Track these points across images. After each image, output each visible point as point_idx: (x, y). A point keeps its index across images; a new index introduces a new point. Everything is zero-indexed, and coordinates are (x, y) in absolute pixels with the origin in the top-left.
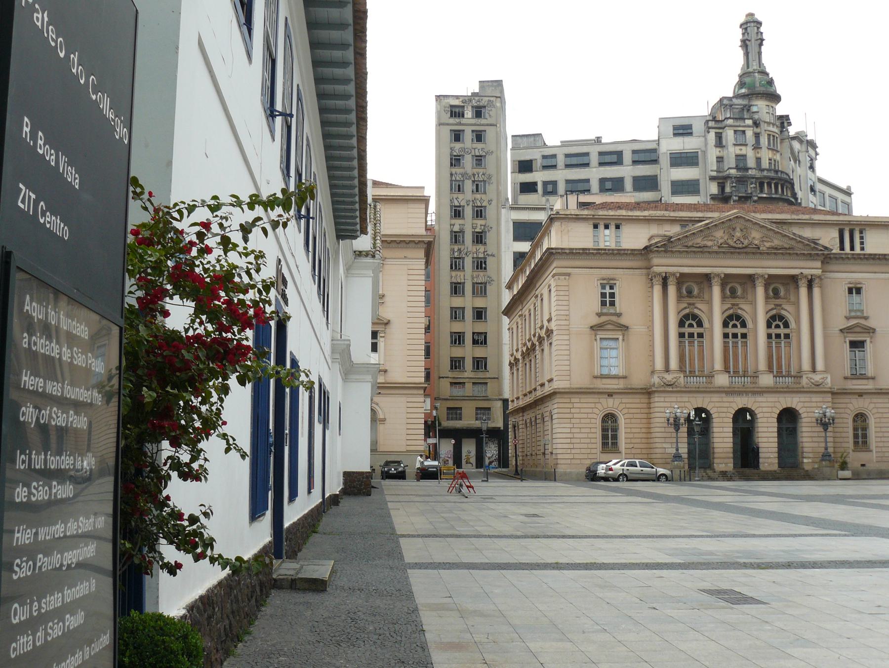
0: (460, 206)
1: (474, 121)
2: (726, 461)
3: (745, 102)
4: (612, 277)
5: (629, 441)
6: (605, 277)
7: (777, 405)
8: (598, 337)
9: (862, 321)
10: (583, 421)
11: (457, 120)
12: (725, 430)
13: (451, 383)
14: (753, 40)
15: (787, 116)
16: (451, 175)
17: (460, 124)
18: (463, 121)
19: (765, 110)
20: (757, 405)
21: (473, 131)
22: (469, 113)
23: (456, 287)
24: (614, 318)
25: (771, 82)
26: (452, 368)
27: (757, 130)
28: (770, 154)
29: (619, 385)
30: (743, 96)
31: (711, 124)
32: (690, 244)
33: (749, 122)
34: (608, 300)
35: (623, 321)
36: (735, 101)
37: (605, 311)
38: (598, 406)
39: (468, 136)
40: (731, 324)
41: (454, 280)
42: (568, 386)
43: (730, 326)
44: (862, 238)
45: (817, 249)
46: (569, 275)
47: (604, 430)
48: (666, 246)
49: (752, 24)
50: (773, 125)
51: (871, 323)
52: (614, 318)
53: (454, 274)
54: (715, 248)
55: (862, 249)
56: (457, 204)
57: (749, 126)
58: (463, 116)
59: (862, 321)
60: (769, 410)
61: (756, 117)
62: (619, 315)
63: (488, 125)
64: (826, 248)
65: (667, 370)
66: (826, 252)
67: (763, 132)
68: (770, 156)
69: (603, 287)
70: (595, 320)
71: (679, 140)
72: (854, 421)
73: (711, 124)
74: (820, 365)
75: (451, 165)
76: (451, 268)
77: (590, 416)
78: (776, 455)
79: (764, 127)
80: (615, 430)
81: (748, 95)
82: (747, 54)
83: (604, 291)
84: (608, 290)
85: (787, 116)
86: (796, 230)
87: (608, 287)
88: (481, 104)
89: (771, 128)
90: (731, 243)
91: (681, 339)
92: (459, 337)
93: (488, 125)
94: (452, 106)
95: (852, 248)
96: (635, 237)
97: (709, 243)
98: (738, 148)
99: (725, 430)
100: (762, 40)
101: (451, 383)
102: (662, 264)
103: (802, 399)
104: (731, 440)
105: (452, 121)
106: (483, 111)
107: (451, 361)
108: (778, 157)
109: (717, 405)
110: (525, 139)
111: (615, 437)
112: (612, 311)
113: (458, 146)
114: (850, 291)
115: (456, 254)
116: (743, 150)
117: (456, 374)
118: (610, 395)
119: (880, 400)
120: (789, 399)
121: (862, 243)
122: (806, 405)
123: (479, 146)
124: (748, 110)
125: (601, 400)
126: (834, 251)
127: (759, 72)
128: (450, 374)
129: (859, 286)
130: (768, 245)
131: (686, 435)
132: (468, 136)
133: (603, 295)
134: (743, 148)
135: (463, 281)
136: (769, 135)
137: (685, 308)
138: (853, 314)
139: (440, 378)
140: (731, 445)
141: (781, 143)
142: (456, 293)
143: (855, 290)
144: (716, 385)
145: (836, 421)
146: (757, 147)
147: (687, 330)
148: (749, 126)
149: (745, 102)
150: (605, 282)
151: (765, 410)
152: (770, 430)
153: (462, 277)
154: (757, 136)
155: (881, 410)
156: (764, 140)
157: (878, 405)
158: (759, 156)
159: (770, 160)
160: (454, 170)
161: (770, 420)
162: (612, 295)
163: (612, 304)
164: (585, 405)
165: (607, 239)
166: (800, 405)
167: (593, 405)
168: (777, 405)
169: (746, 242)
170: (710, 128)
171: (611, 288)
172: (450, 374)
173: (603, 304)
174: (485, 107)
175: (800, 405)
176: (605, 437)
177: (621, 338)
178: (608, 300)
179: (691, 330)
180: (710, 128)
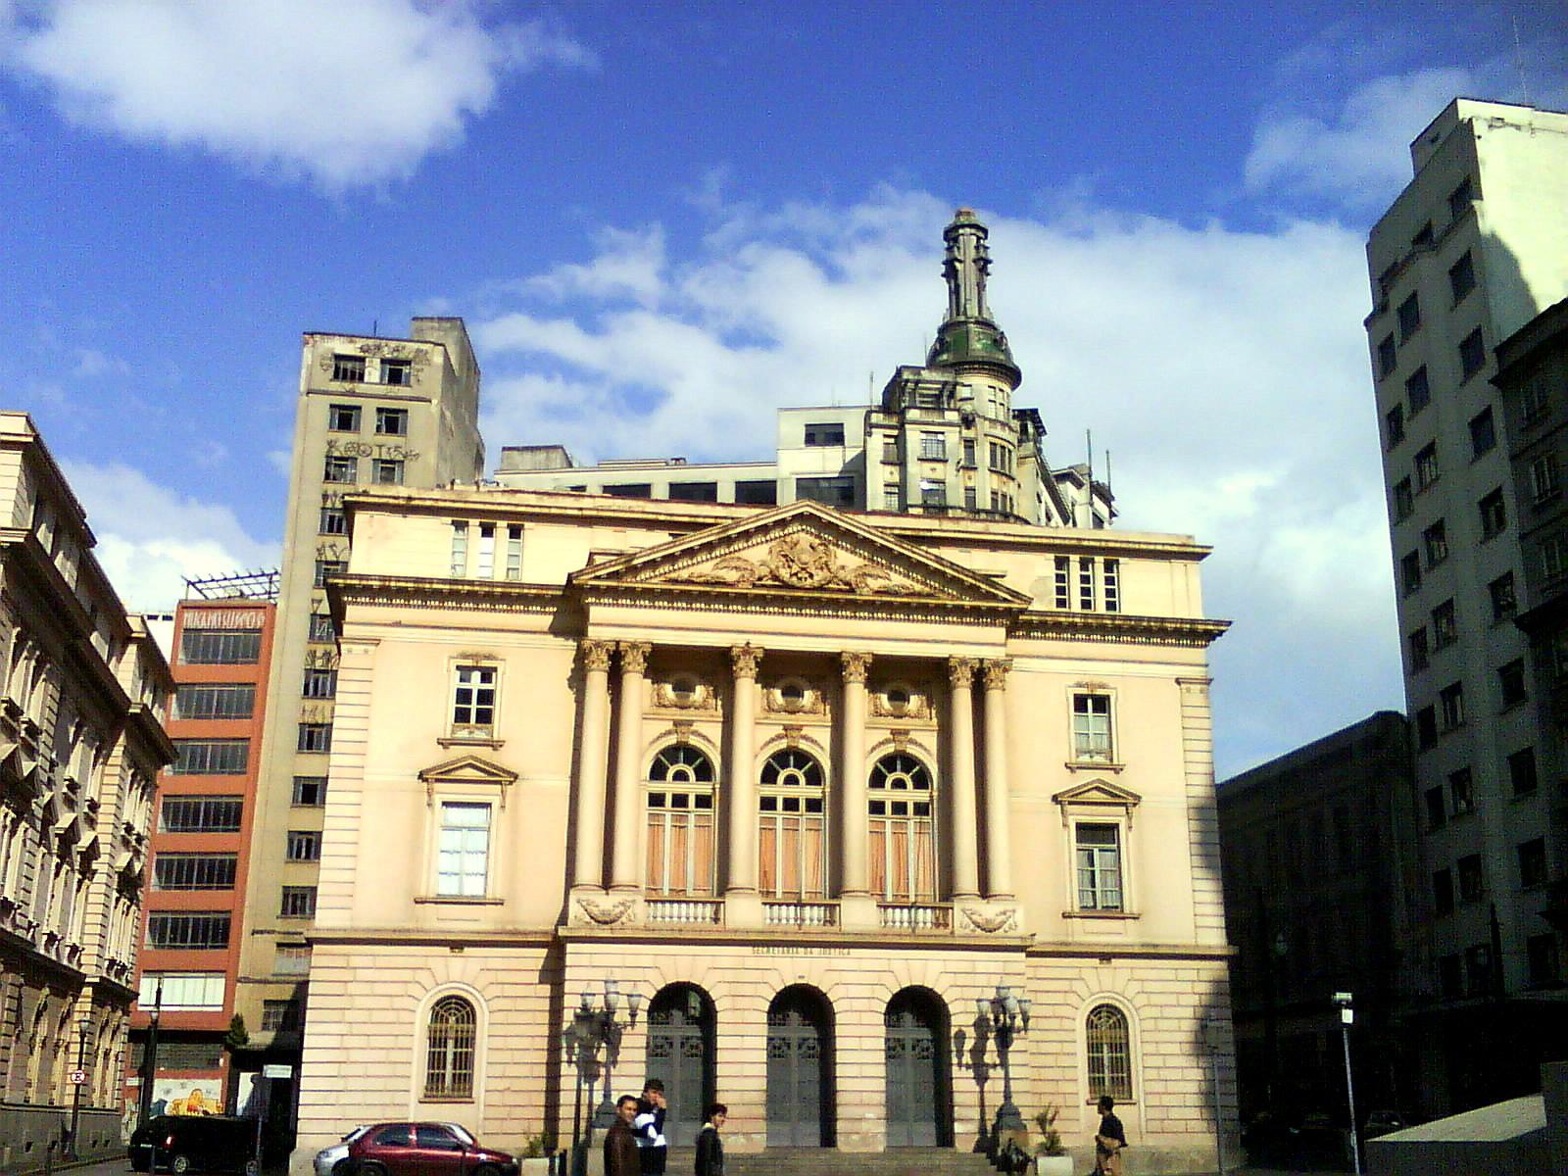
0: (337, 563)
1: (383, 389)
2: (748, 1127)
3: (948, 377)
4: (486, 651)
5: (498, 1070)
6: (470, 650)
7: (887, 979)
8: (438, 799)
9: (1108, 777)
10: (377, 1016)
11: (347, 386)
12: (749, 1042)
13: (279, 945)
14: (969, 261)
15: (1035, 411)
16: (325, 497)
17: (352, 394)
18: (360, 388)
19: (989, 394)
20: (835, 977)
21: (380, 410)
22: (373, 372)
23: (311, 734)
24: (485, 753)
25: (998, 341)
26: (284, 910)
27: (966, 433)
28: (994, 482)
29: (482, 921)
30: (944, 367)
31: (876, 418)
32: (684, 574)
33: (952, 416)
34: (475, 707)
35: (504, 759)
36: (926, 375)
37: (463, 734)
38: (423, 977)
39: (369, 419)
40: (783, 775)
41: (309, 720)
42: (347, 924)
43: (781, 778)
44: (1109, 581)
45: (995, 597)
46: (376, 642)
47: (437, 1041)
48: (622, 581)
49: (968, 230)
50: (1004, 424)
51: (1126, 782)
52: (485, 753)
53: (309, 704)
54: (744, 589)
55: (1111, 606)
56: (331, 557)
57: (951, 424)
58: (361, 378)
59: (1108, 777)
60: (866, 991)
61: (967, 407)
62: (496, 745)
63: (411, 399)
64: (1016, 594)
65: (607, 883)
66: (1016, 605)
67: (981, 438)
68: (995, 487)
69: (465, 672)
70: (436, 757)
71: (816, 452)
72: (1090, 1024)
73: (876, 418)
74: (1000, 882)
75: (327, 476)
76: (306, 692)
77: (398, 1003)
78: (882, 1112)
79: (983, 427)
80: (466, 1041)
81: (952, 365)
82: (955, 292)
83: (465, 686)
84: (475, 683)
85: (1035, 411)
86: (949, 554)
87: (476, 676)
88: (402, 356)
89: (998, 431)
90: (784, 574)
91: (656, 810)
92: (309, 842)
93: (411, 399)
94: (339, 357)
95: (1086, 604)
96: (552, 556)
97: (731, 576)
98: (928, 466)
99: (749, 1042)
100: (988, 262)
101: (279, 945)
102: (608, 621)
103: (952, 967)
104: (763, 1070)
105: (337, 386)
106: (406, 370)
107: (286, 896)
108: (1010, 489)
109: (729, 976)
110: (528, 455)
111: (464, 1061)
112: (480, 735)
113: (345, 438)
114: (1080, 703)
115: (319, 664)
116: (940, 471)
117: (293, 924)
118: (457, 945)
119: (1153, 974)
120: (916, 966)
121: (1110, 593)
122: (961, 980)
123: (392, 440)
124: (952, 395)
125: (431, 963)
126: (1035, 606)
127: (977, 322)
128: (280, 925)
129: (1100, 692)
130: (875, 584)
131: (642, 1055)
132: (369, 419)
133: (463, 696)
134: (939, 466)
135: (327, 721)
136: (993, 444)
137: (669, 733)
138: (1085, 759)
139: (254, 932)
140: (763, 1084)
141: (1019, 464)
142: (310, 747)
143: (1093, 703)
144: (730, 925)
145: (1031, 1023)
146: (970, 467)
147: (669, 787)
148: (951, 424)
149: (948, 377)
150: (469, 663)
151: (854, 991)
152: (868, 1043)
153: (328, 713)
154: (969, 444)
155: (1156, 999)
156: (983, 454)
157: (1150, 987)
158: (970, 484)
159: (994, 493)
160: (331, 488)
161: (866, 1018)
162: (486, 697)
163: (485, 717)
164: (387, 975)
165: (485, 558)
166: (948, 980)
167: (406, 975)
168: (887, 979)
169: (820, 576)
170: (872, 426)
171: (487, 676)
172: (280, 925)
173: (462, 716)
174: (408, 363)
175: (948, 980)
176: (436, 1061)
177: (496, 802)
178: (475, 707)
179: (680, 788)
180: (872, 426)
